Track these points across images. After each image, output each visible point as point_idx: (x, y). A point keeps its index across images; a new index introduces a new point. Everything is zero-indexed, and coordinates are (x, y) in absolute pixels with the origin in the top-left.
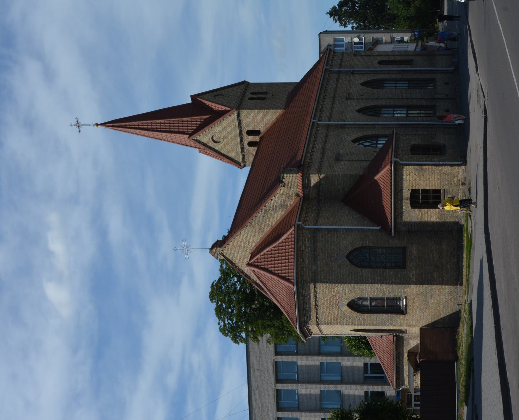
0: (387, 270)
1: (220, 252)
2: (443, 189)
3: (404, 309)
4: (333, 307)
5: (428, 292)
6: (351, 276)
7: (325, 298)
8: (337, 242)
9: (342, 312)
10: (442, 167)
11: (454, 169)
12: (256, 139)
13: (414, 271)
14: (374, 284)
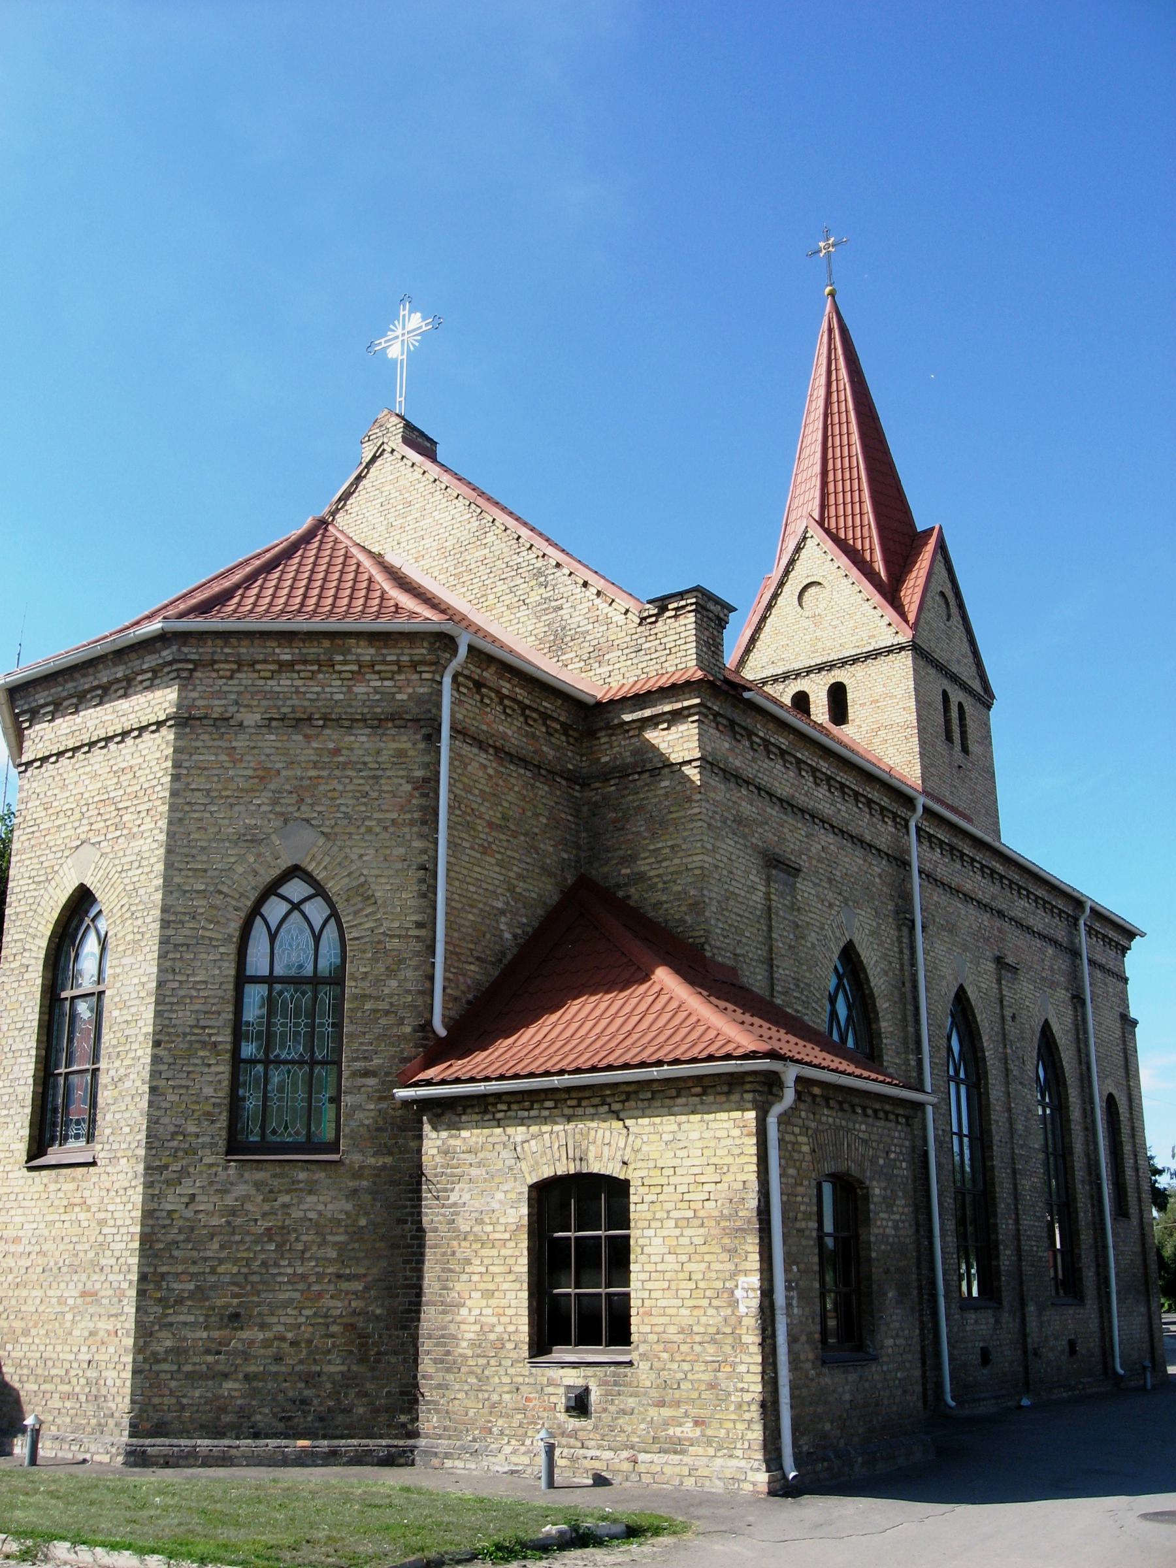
0: (221, 1068)
1: (385, 446)
2: (634, 1356)
3: (49, 1160)
4: (76, 824)
5: (111, 1277)
6: (203, 887)
7: (116, 780)
8: (374, 823)
9: (56, 868)
10: (755, 1349)
11: (750, 1421)
12: (820, 710)
13: (211, 1207)
14: (157, 1003)
